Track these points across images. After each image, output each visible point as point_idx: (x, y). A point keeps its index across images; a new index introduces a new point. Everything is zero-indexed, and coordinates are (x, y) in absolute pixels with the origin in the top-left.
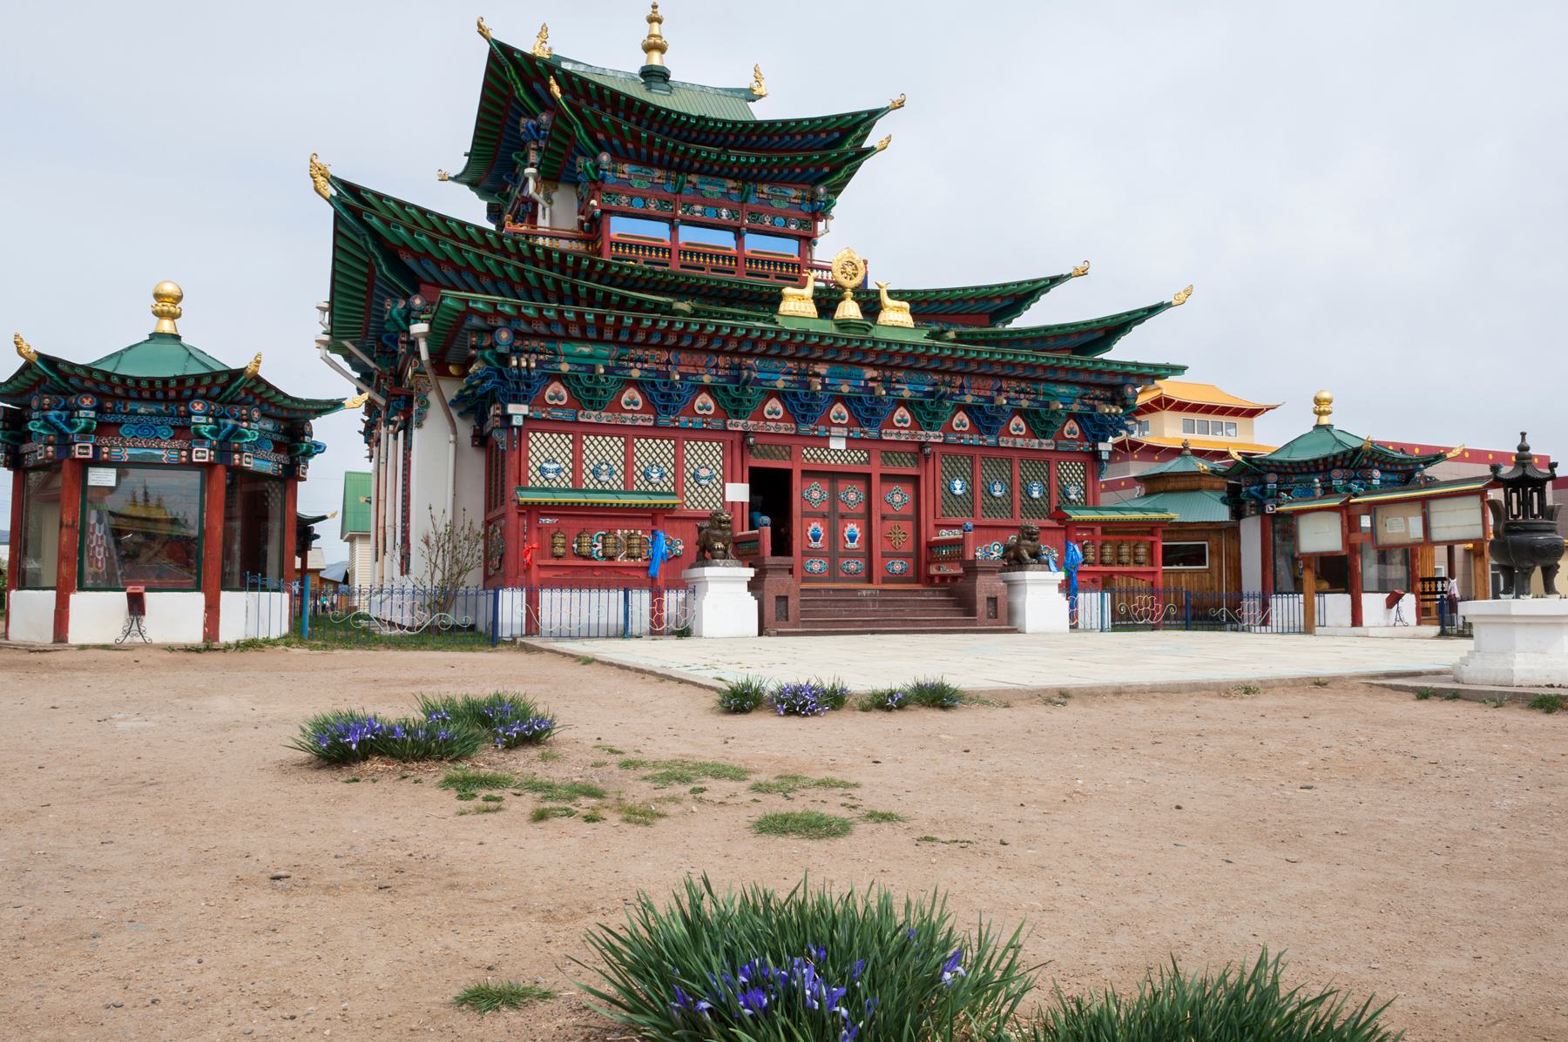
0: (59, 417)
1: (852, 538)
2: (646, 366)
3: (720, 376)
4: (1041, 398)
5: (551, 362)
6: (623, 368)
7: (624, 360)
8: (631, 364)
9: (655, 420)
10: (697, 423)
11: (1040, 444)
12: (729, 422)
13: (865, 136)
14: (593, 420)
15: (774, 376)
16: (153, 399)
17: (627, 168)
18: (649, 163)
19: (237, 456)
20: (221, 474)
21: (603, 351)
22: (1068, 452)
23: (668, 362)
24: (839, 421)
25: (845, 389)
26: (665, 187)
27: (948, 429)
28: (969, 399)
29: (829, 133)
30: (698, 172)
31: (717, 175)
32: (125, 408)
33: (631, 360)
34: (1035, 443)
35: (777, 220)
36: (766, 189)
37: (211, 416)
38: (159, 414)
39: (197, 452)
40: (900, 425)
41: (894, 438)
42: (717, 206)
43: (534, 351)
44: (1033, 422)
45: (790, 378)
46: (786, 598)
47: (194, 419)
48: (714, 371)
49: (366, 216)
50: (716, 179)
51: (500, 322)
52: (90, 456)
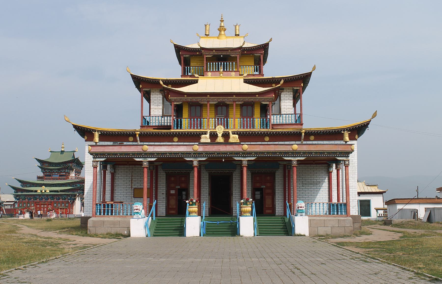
17: (46, 170)
28: (55, 197)
42: (56, 172)
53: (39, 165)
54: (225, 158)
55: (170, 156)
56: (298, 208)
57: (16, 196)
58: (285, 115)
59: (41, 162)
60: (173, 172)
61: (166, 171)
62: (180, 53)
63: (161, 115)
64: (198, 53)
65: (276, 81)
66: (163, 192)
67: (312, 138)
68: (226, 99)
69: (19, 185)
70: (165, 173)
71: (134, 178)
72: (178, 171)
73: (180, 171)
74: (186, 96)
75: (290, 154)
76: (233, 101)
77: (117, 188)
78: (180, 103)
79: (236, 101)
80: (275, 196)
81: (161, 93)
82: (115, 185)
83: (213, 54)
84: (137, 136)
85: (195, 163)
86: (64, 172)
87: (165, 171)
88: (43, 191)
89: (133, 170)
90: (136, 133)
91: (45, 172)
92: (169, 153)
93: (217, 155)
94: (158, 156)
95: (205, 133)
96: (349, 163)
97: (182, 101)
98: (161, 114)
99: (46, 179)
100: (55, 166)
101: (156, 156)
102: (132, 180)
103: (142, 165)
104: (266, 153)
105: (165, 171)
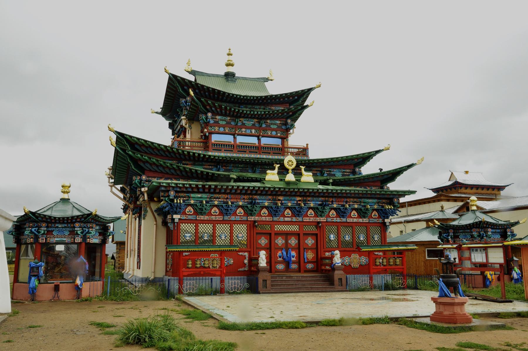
0: (35, 230)
1: (293, 257)
2: (219, 200)
3: (245, 202)
4: (363, 204)
5: (188, 200)
6: (212, 201)
7: (212, 198)
8: (215, 200)
9: (223, 218)
10: (238, 218)
11: (363, 220)
12: (248, 217)
13: (304, 101)
14: (202, 219)
15: (264, 201)
16: (63, 223)
17: (218, 117)
18: (225, 115)
19: (88, 239)
20: (83, 245)
21: (204, 196)
22: (374, 223)
23: (227, 198)
24: (288, 215)
25: (290, 204)
26: (231, 123)
27: (328, 216)
29: (293, 97)
30: (244, 117)
31: (250, 118)
32: (55, 226)
33: (215, 198)
34: (361, 220)
35: (273, 132)
36: (268, 121)
37: (81, 228)
38: (65, 227)
39: (77, 239)
40: (310, 216)
41: (308, 220)
42: (250, 128)
43: (182, 197)
44: (360, 212)
45: (270, 201)
46: (266, 280)
47: (76, 229)
48: (243, 200)
49: (127, 151)
50: (250, 119)
51: (171, 189)
52: (44, 242)
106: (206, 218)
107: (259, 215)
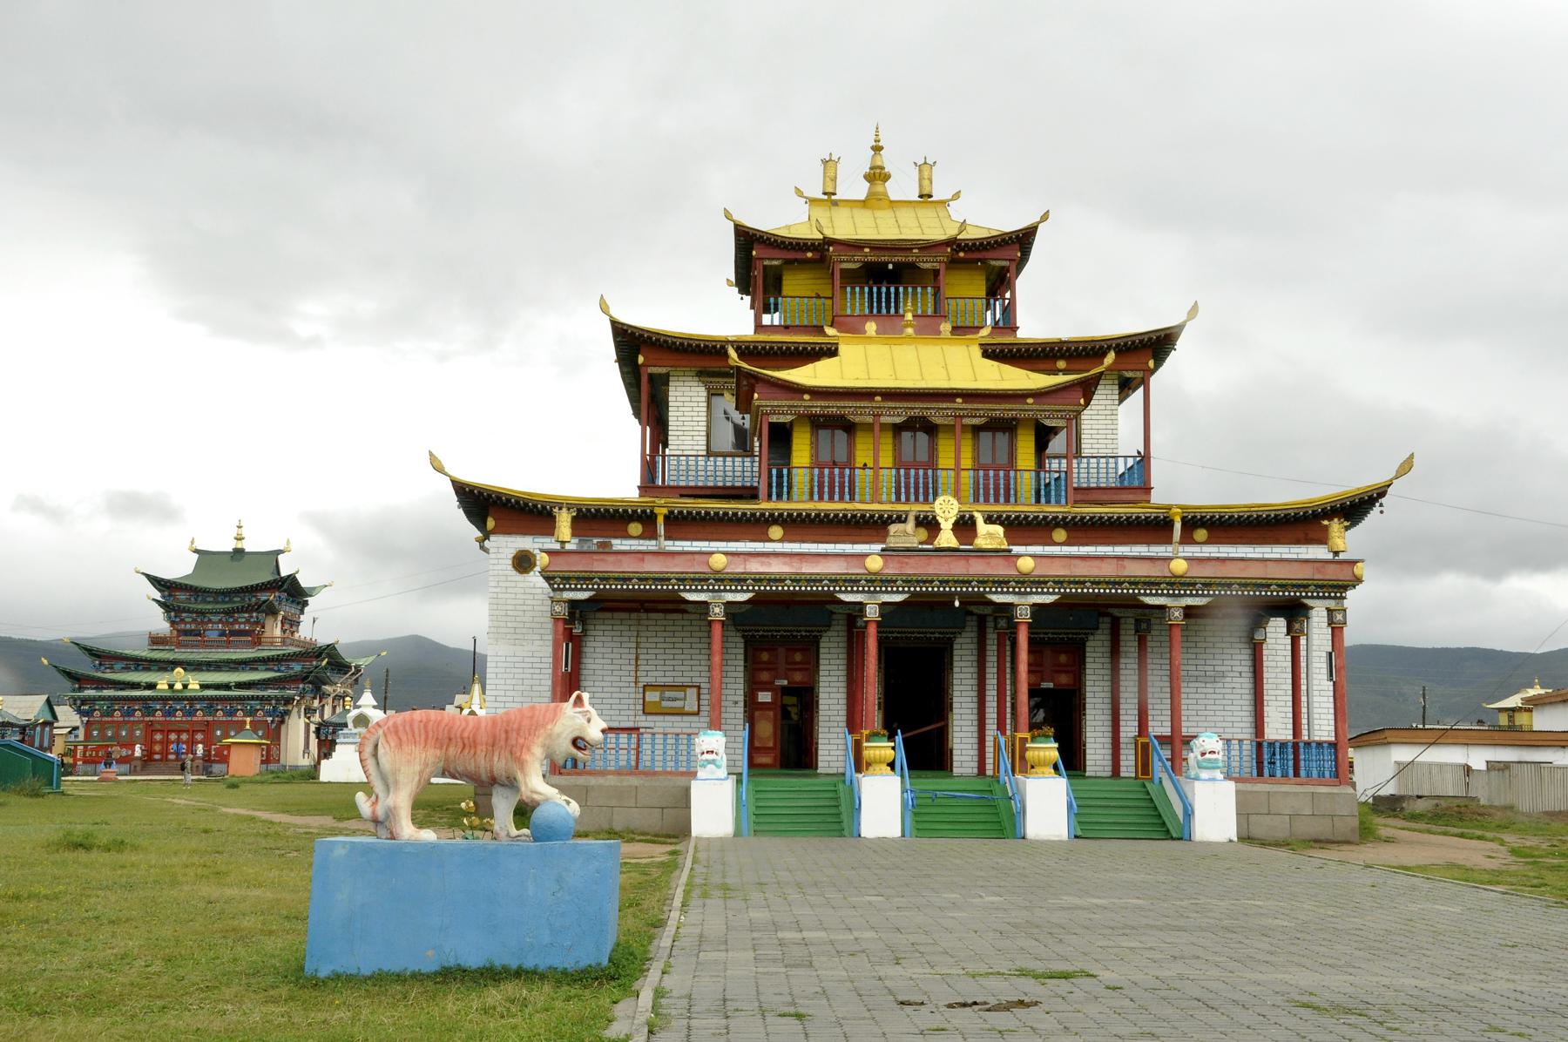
10: (136, 719)
17: (184, 615)
53: (158, 596)
54: (961, 594)
55: (794, 587)
56: (1203, 754)
57: (79, 702)
58: (1095, 460)
59: (162, 586)
60: (767, 636)
61: (746, 631)
62: (754, 253)
63: (704, 453)
64: (809, 255)
65: (1082, 353)
66: (736, 698)
67: (1201, 534)
68: (934, 409)
69: (86, 667)
70: (743, 637)
71: (645, 651)
72: (785, 631)
73: (791, 631)
74: (806, 397)
75: (1162, 586)
76: (955, 416)
77: (592, 684)
78: (789, 418)
79: (962, 417)
80: (1085, 714)
81: (703, 382)
82: (584, 672)
83: (864, 262)
84: (660, 520)
85: (872, 612)
86: (248, 621)
87: (743, 631)
88: (178, 686)
89: (640, 628)
90: (657, 510)
91: (178, 620)
92: (793, 577)
93: (939, 588)
94: (757, 588)
95: (901, 519)
96: (1345, 617)
97: (795, 414)
98: (702, 451)
99: (180, 645)
100: (212, 599)
101: (751, 588)
102: (637, 659)
103: (707, 614)
104: (1088, 584)
105: (743, 631)
106: (110, 719)
107: (154, 716)
